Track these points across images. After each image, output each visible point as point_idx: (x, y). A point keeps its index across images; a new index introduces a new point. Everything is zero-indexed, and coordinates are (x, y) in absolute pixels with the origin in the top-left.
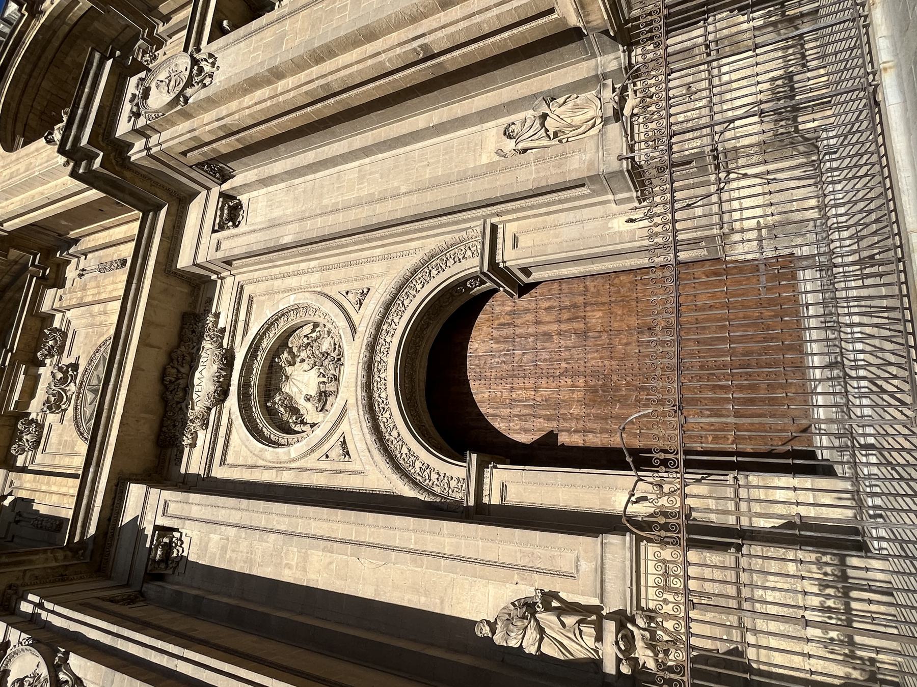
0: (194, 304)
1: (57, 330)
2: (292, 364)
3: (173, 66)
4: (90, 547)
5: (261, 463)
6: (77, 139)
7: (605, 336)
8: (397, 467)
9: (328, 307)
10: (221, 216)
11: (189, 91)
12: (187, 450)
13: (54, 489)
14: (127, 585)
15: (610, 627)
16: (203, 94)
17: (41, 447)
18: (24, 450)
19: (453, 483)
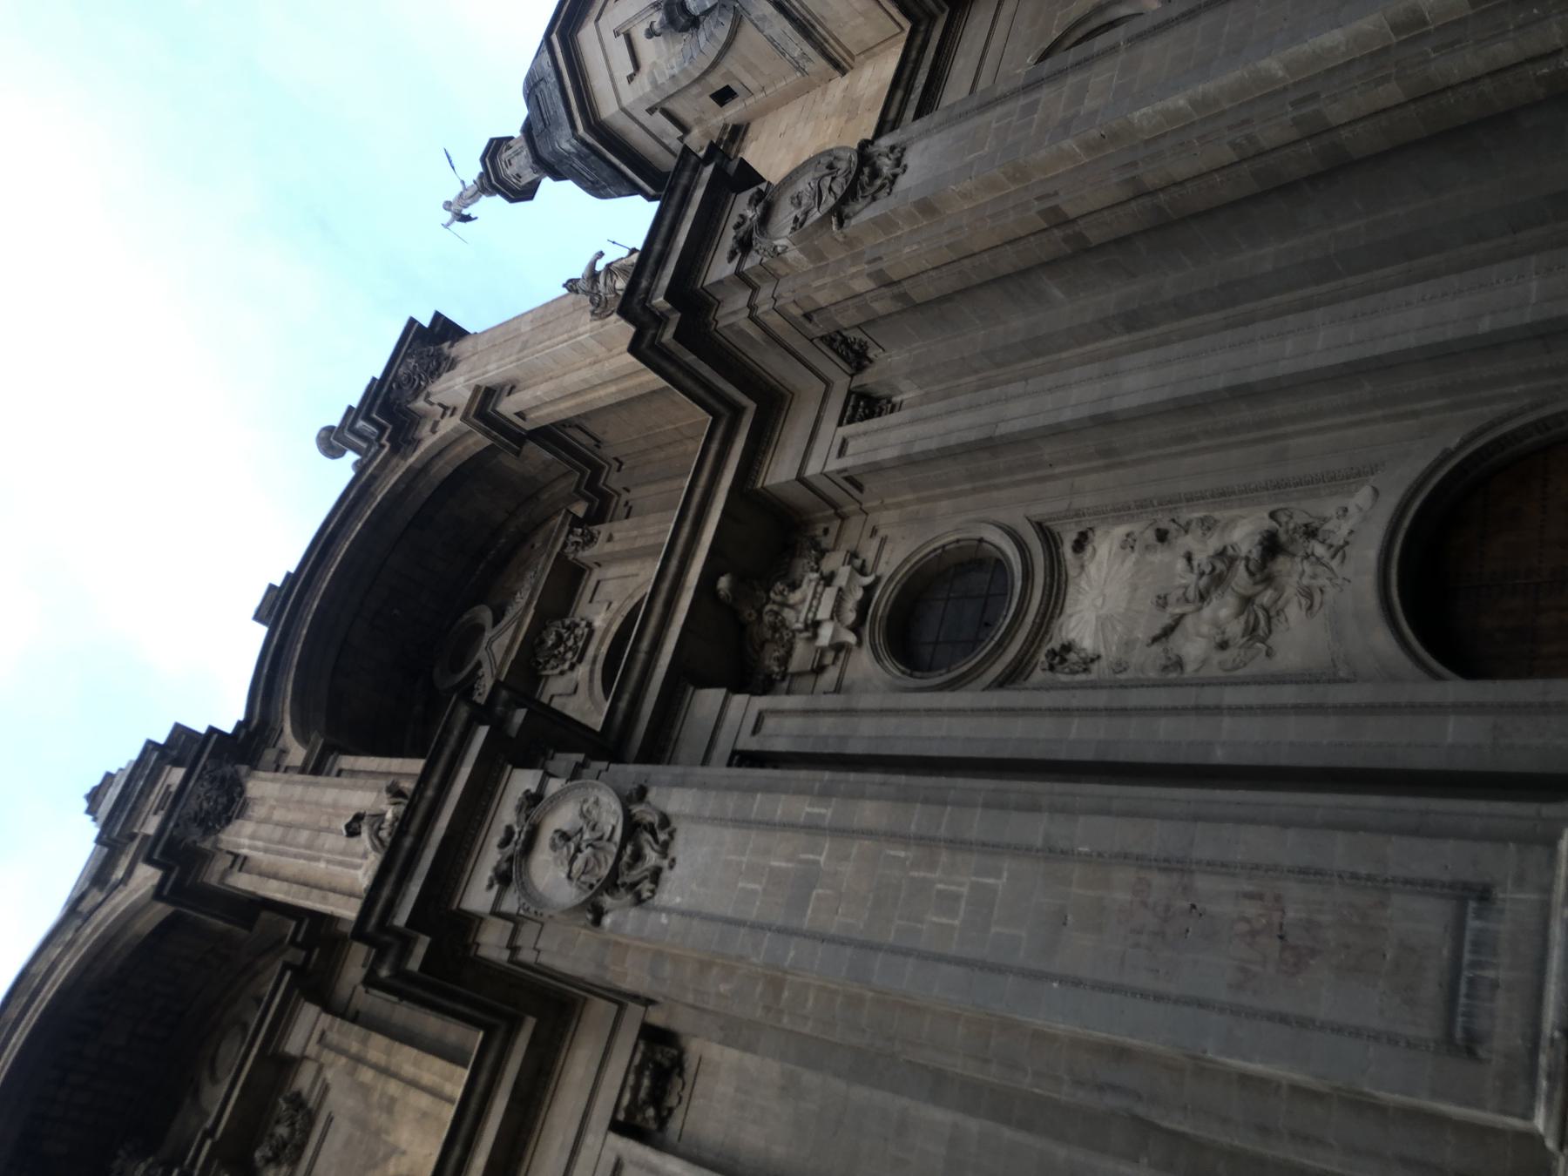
3: (592, 800)
6: (391, 907)
10: (636, 1089)
11: (607, 901)
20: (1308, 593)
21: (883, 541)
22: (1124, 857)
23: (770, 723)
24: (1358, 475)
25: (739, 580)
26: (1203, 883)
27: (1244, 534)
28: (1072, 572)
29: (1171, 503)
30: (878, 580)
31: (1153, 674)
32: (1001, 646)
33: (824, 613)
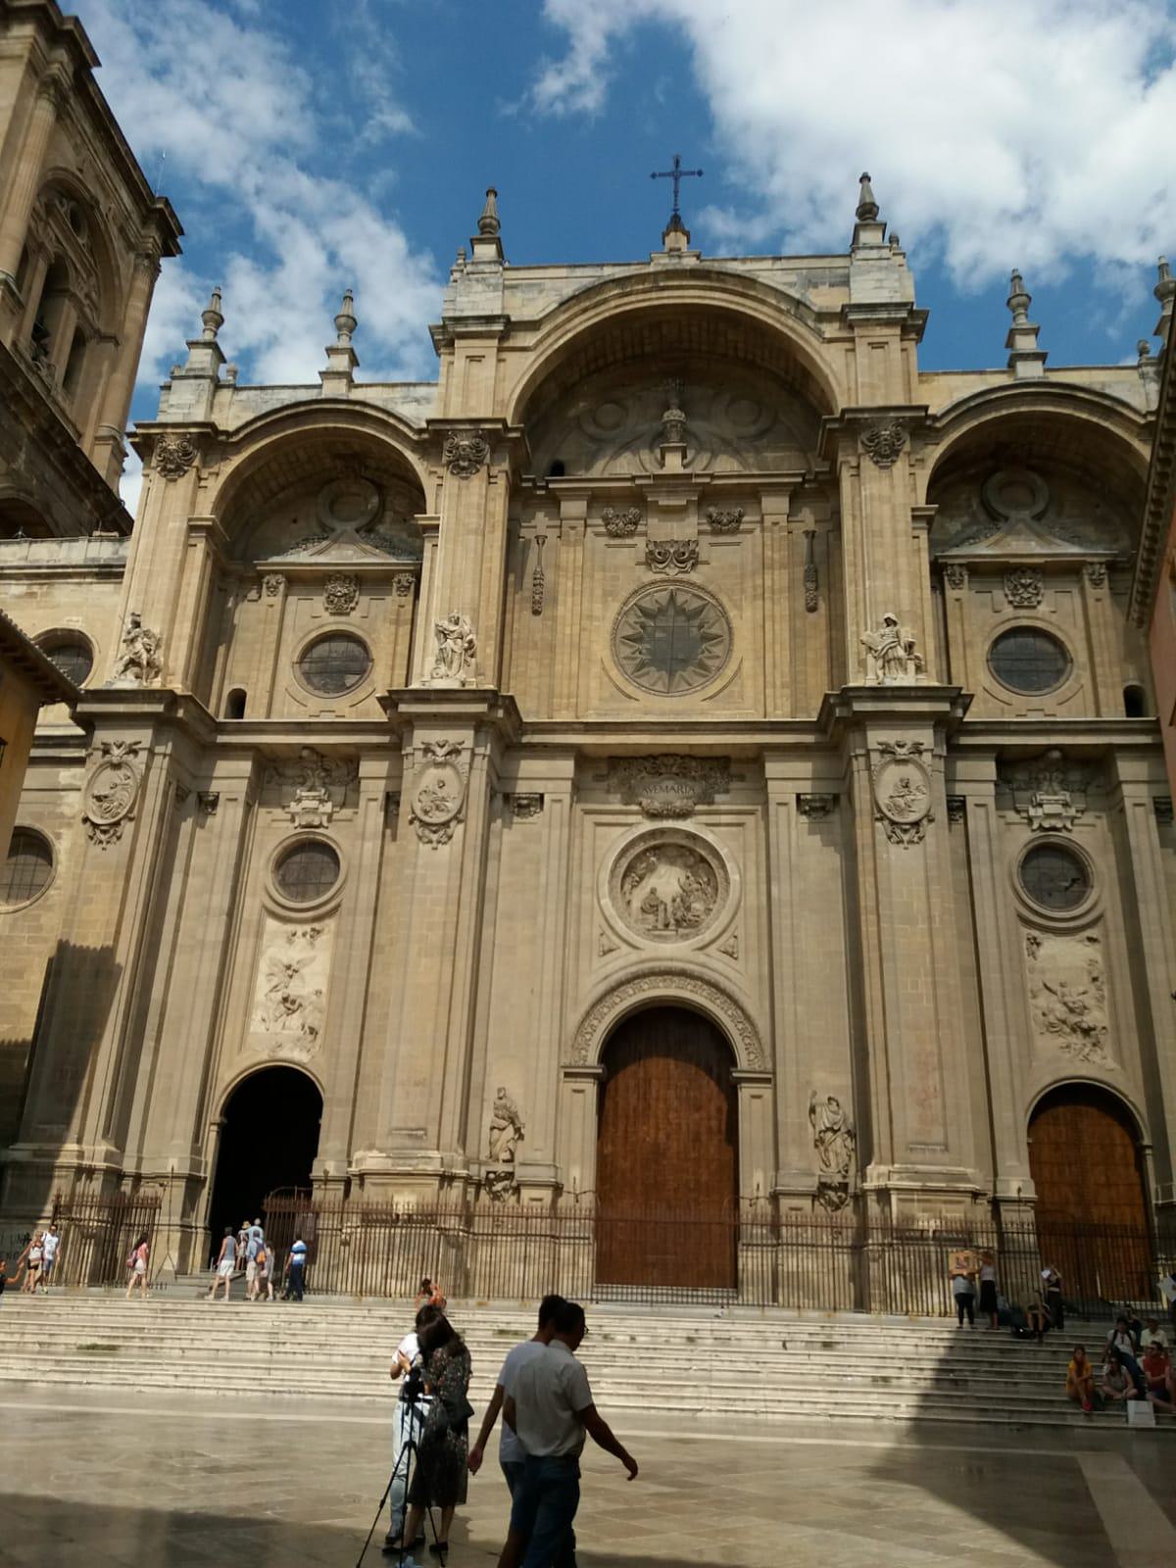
0: (740, 761)
1: (741, 515)
2: (687, 866)
4: (525, 739)
5: (597, 865)
6: (860, 698)
7: (693, 1155)
8: (594, 1006)
9: (724, 918)
11: (886, 822)
12: (604, 785)
13: (569, 600)
14: (499, 778)
15: (510, 1170)
16: (881, 837)
17: (612, 542)
18: (606, 525)
19: (583, 1052)
20: (1068, 1047)
21: (1094, 826)
22: (940, 1048)
23: (981, 811)
24: (1122, 1063)
25: (1058, 760)
26: (937, 1075)
27: (1096, 1017)
28: (1078, 937)
29: (1111, 982)
30: (1070, 831)
31: (1029, 986)
32: (1036, 913)
33: (1048, 809)
